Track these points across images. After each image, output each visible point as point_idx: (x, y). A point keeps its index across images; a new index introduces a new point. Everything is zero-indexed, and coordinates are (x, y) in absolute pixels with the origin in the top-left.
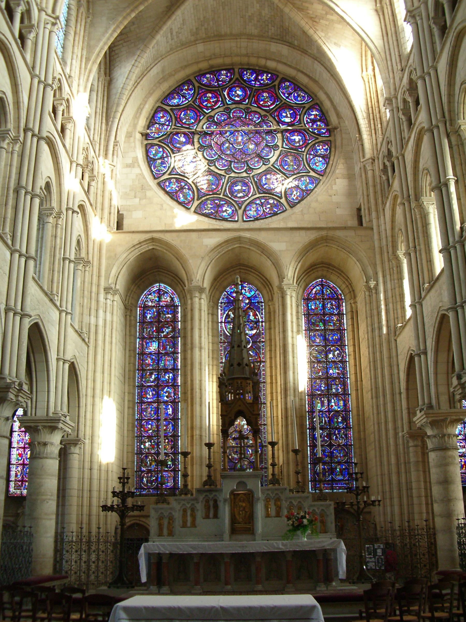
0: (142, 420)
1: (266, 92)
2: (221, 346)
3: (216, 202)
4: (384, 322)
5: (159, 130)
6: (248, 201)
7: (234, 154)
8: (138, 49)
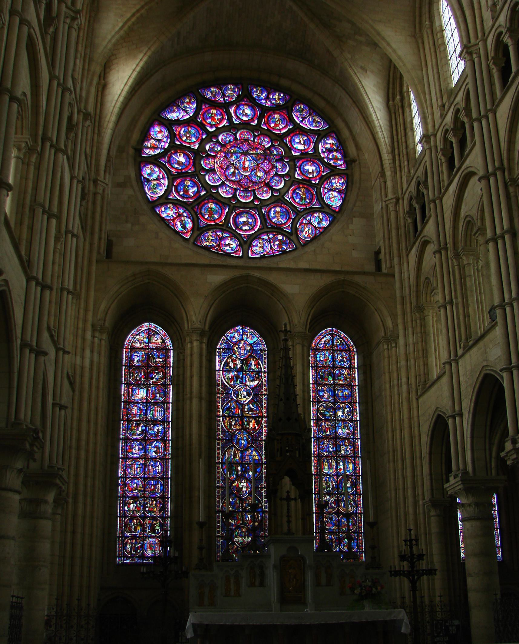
0: (126, 478)
1: (277, 113)
2: (219, 397)
3: (219, 233)
5: (154, 148)
6: (254, 236)
7: (240, 180)
8: (141, 52)
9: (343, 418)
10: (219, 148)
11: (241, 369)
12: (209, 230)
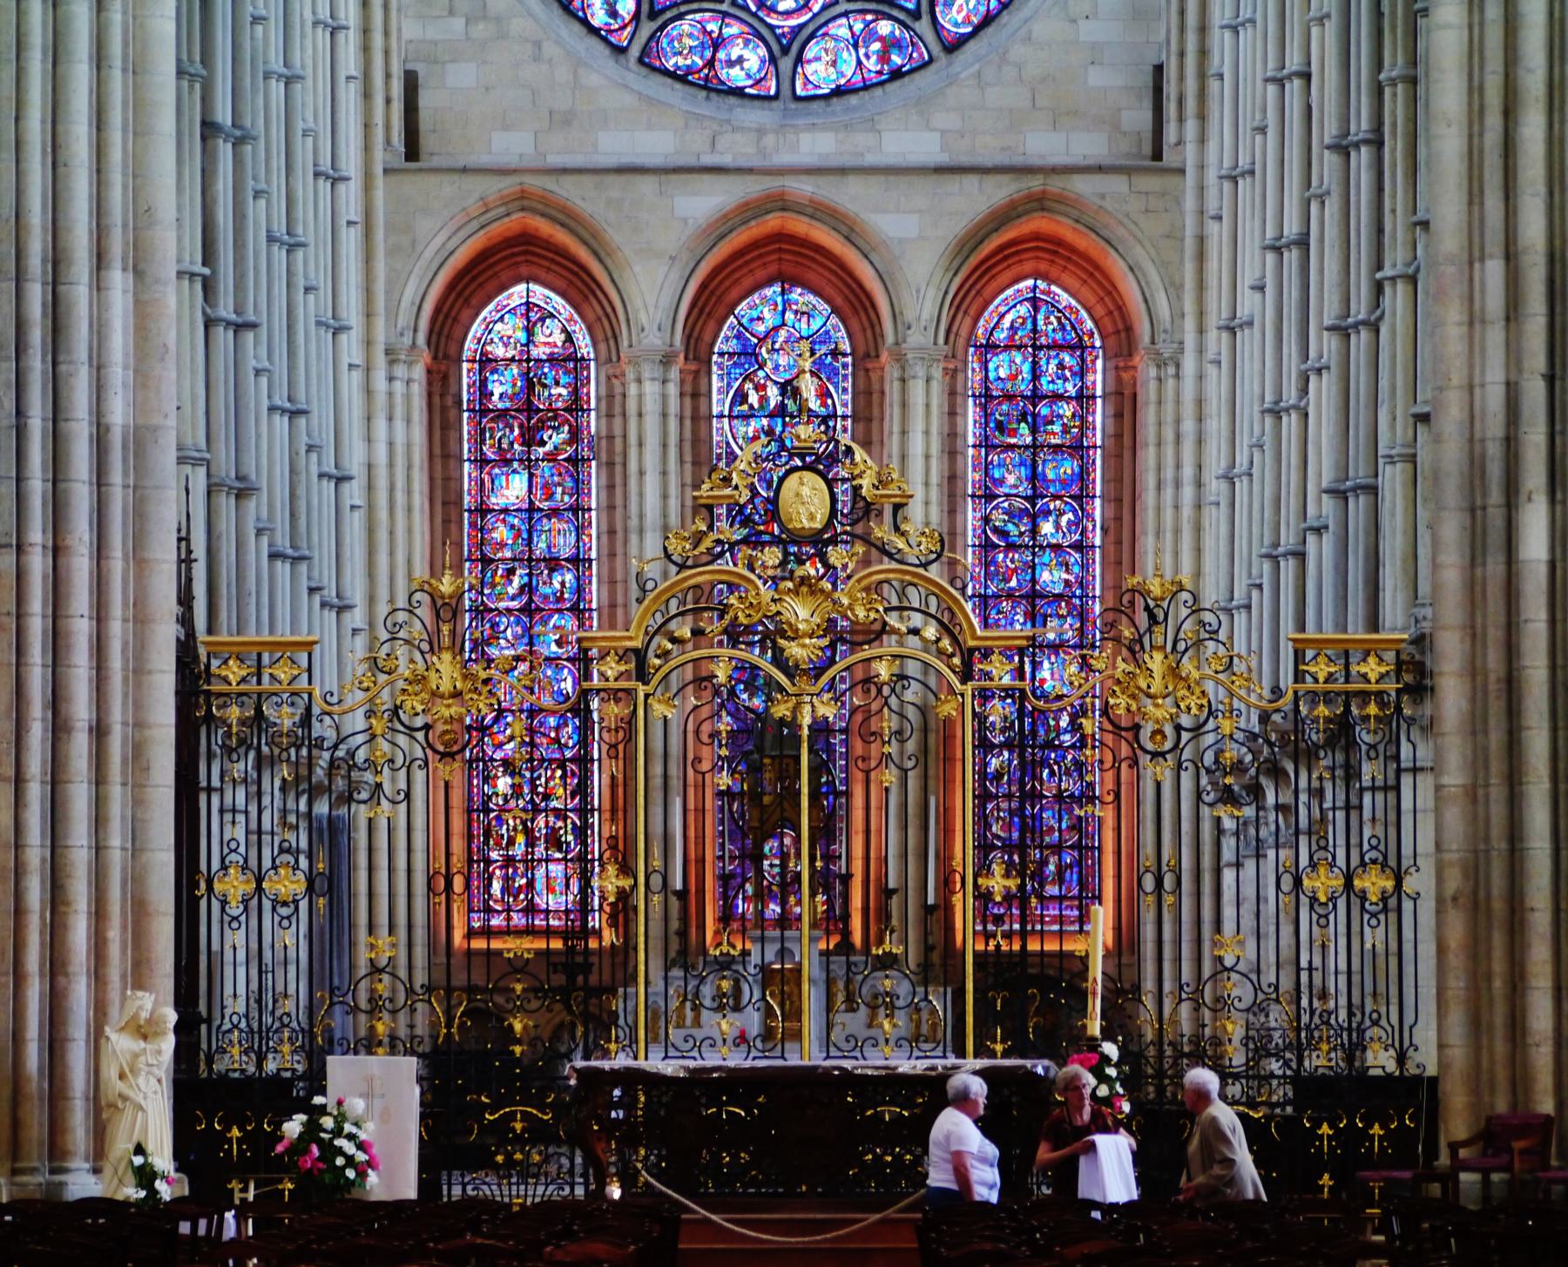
3: (712, 27)
4: (1188, 472)
9: (1054, 541)
11: (781, 411)
12: (680, 17)
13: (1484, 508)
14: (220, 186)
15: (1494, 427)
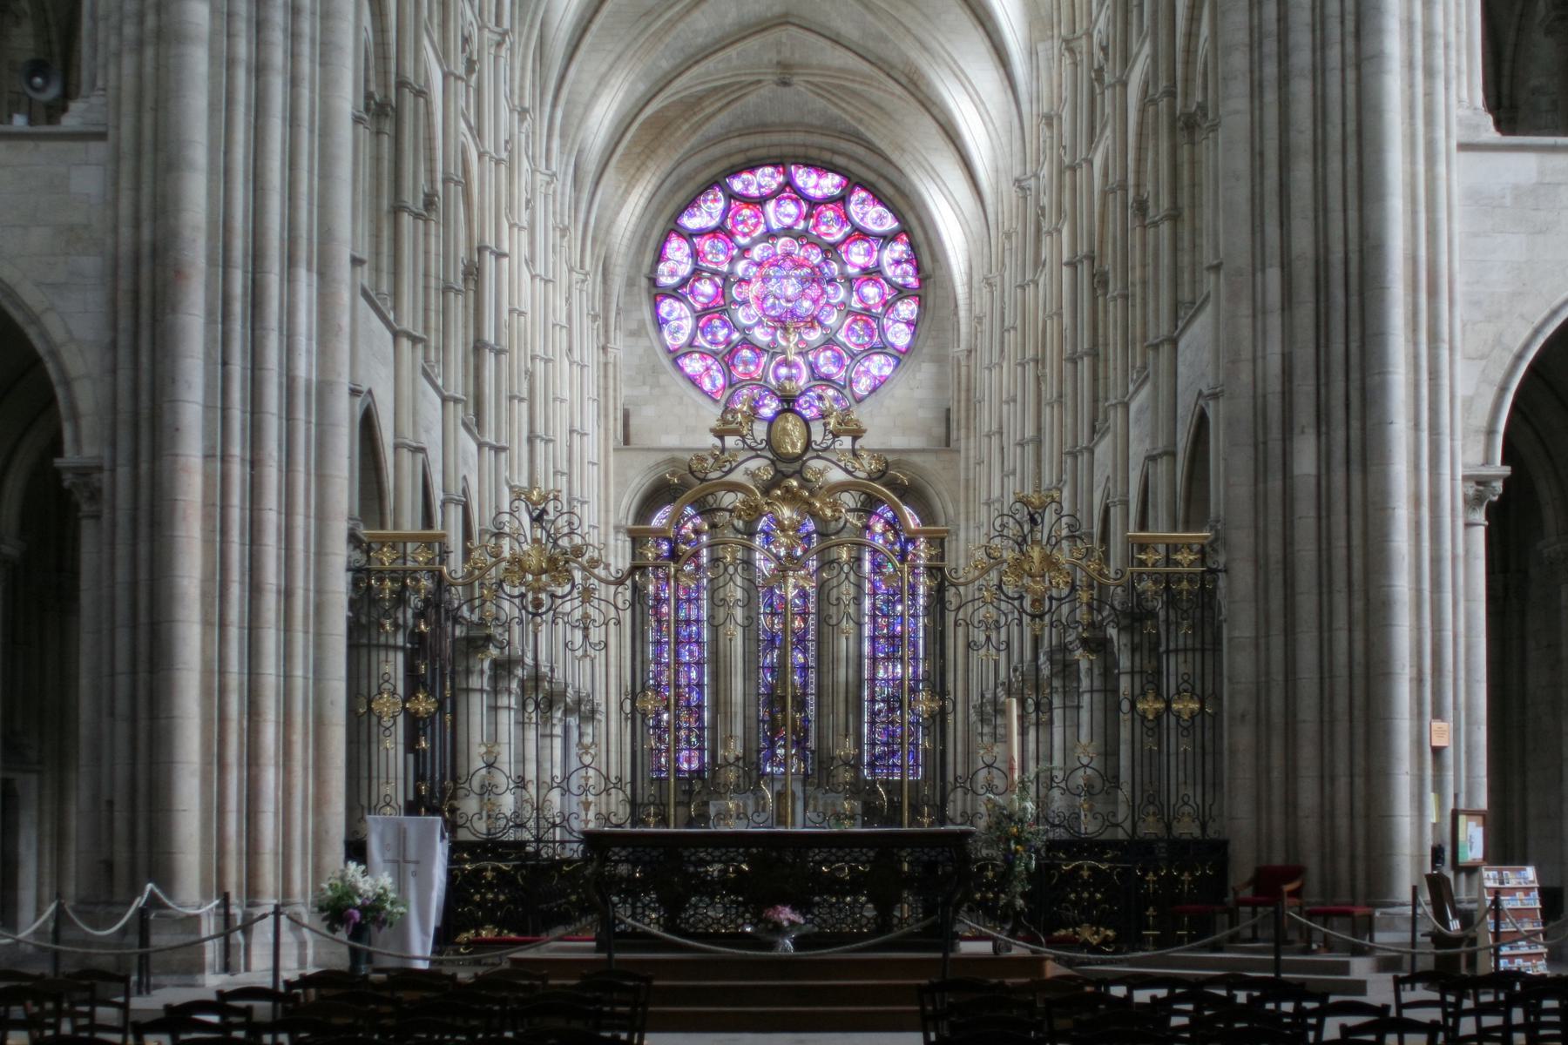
5: (673, 273)
10: (755, 269)
12: (743, 387)
13: (1265, 443)
14: (487, 373)
15: (1275, 385)
